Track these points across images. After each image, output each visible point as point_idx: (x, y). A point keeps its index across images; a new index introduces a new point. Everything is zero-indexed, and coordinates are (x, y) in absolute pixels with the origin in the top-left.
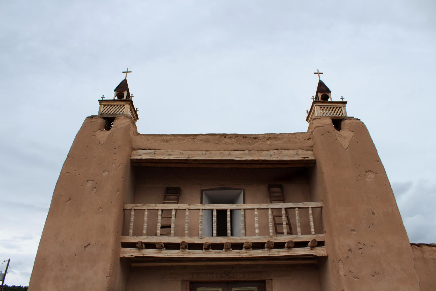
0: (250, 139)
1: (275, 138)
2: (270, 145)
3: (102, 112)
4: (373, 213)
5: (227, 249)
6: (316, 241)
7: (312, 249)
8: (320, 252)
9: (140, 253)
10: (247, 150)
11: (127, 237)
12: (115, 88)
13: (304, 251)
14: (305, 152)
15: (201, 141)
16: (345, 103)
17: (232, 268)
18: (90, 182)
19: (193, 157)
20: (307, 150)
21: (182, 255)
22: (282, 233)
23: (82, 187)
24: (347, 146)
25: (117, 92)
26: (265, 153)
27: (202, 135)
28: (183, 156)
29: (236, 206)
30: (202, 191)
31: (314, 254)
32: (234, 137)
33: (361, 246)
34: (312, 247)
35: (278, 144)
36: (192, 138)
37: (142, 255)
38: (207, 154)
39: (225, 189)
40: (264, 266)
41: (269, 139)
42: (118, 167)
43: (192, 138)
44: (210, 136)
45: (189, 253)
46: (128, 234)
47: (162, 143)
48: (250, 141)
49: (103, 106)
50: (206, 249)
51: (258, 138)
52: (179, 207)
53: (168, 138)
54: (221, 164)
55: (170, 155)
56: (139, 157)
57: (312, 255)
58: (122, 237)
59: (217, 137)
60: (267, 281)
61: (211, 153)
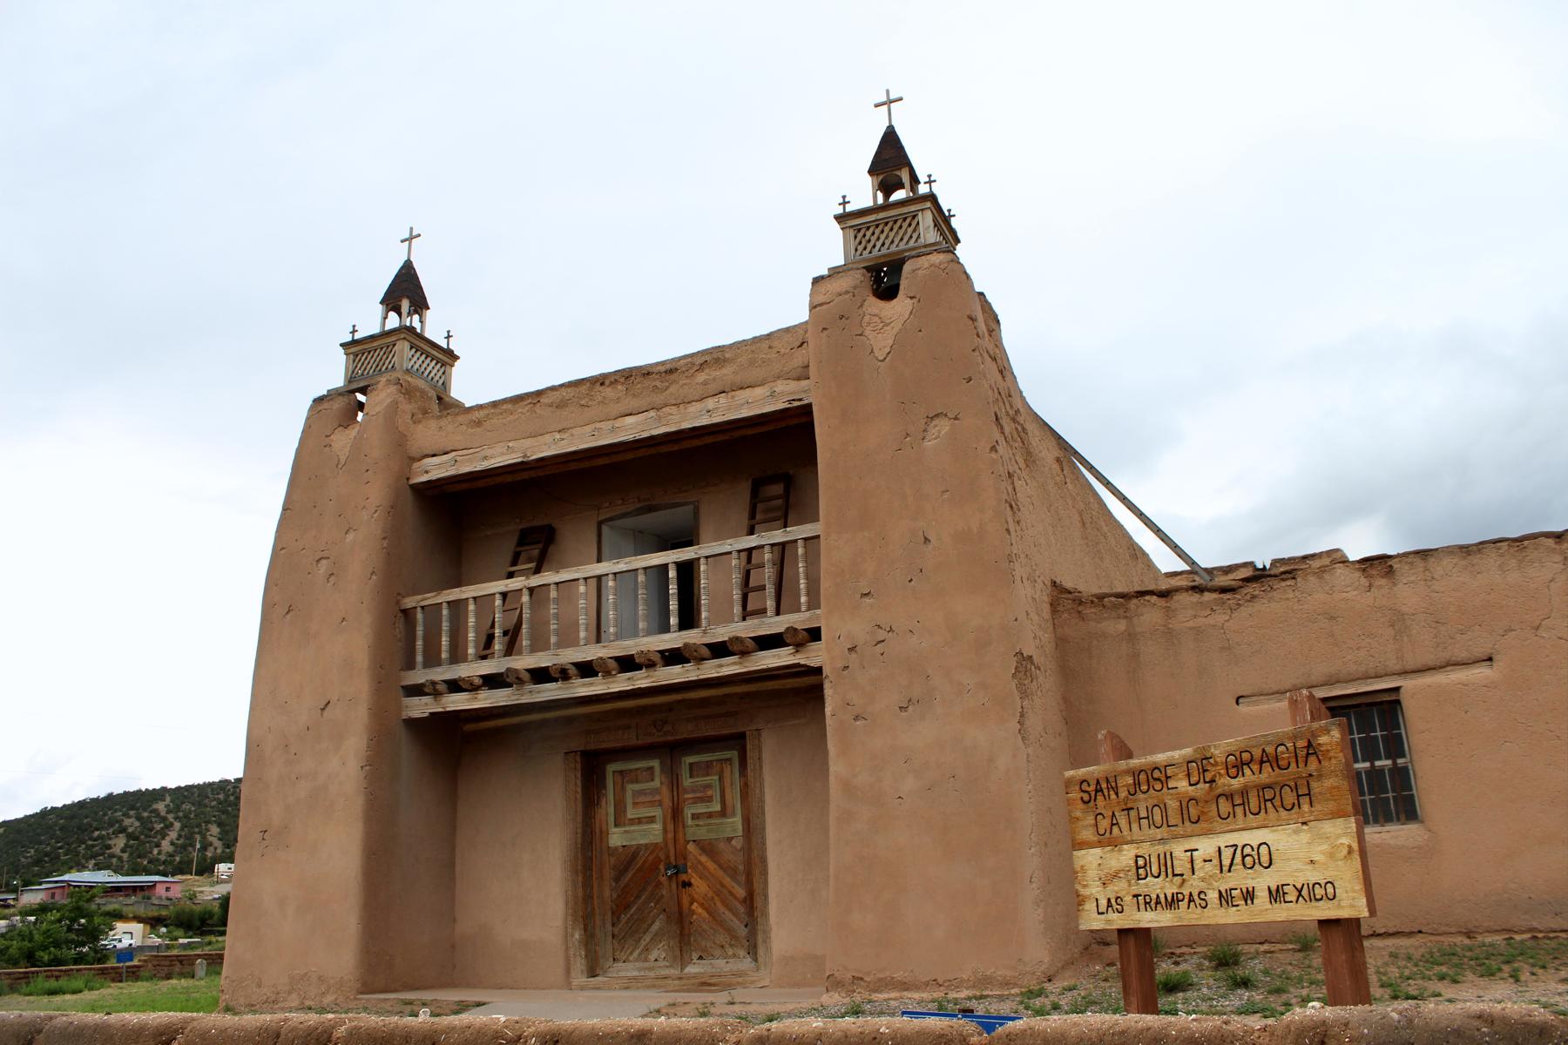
0: (658, 376)
1: (717, 360)
2: (705, 383)
3: (353, 372)
4: (926, 539)
5: (608, 673)
6: (796, 630)
7: (797, 651)
9: (438, 705)
10: (652, 409)
11: (411, 673)
12: (380, 300)
13: (779, 659)
14: (793, 386)
15: (550, 405)
17: (671, 710)
18: (324, 561)
19: (534, 453)
20: (799, 379)
21: (517, 700)
22: (762, 612)
23: (310, 576)
24: (887, 350)
25: (387, 305)
26: (694, 408)
27: (553, 389)
28: (514, 456)
29: (626, 563)
30: (600, 524)
31: (802, 662)
32: (622, 380)
33: (881, 635)
34: (799, 646)
35: (725, 375)
36: (530, 403)
37: (441, 710)
38: (563, 439)
39: (650, 509)
40: (743, 696)
41: (702, 367)
42: (372, 517)
43: (530, 403)
44: (569, 390)
45: (530, 692)
46: (410, 665)
47: (470, 430)
48: (658, 383)
49: (352, 356)
51: (676, 369)
52: (506, 586)
53: (482, 413)
54: (607, 455)
55: (485, 458)
56: (424, 478)
57: (798, 665)
58: (403, 673)
59: (583, 389)
60: (748, 733)
61: (572, 435)
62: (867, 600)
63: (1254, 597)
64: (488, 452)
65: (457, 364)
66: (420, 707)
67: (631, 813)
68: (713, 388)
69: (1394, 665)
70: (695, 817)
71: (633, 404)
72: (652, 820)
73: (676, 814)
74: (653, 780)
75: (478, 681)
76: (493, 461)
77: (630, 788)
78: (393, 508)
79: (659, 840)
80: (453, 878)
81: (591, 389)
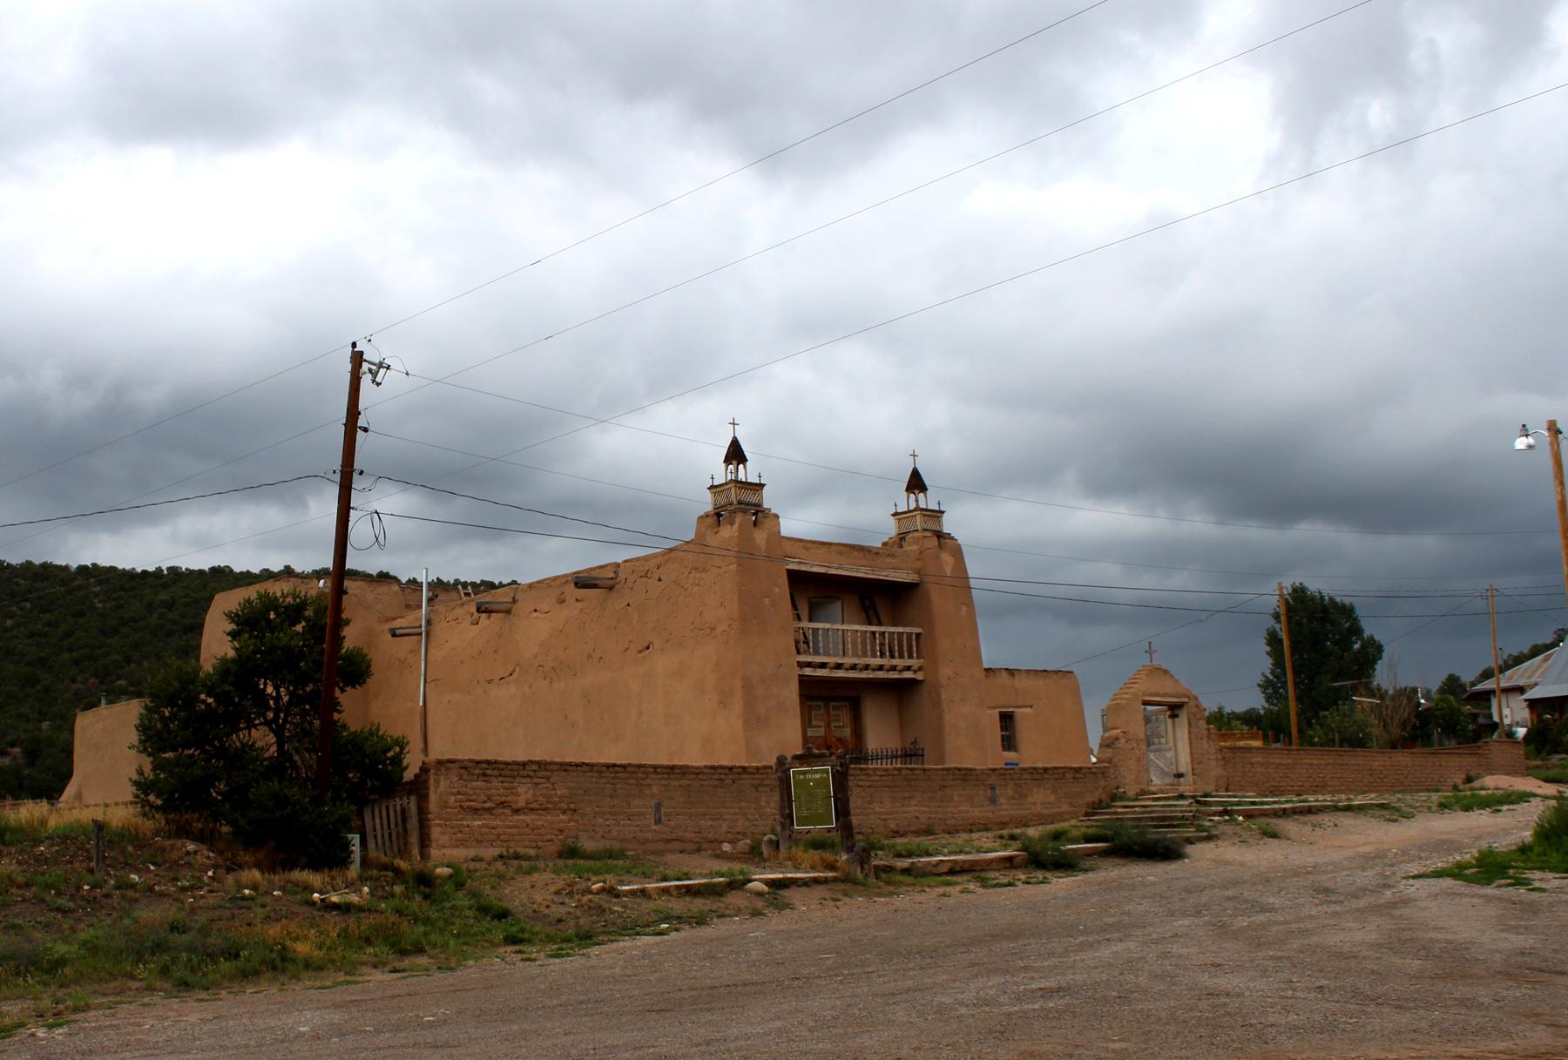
8: (919, 676)
16: (943, 512)
34: (915, 672)
50: (847, 669)
67: (814, 723)
68: (890, 566)
70: (835, 727)
71: (864, 562)
72: (820, 726)
73: (829, 725)
74: (820, 710)
77: (813, 713)
79: (823, 734)
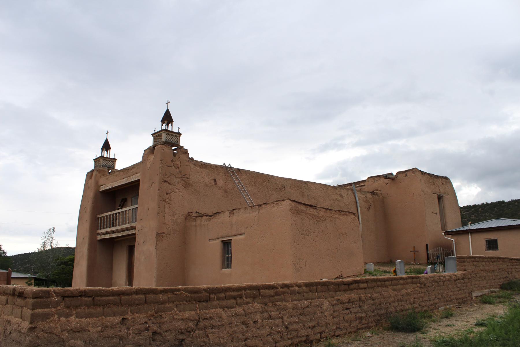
33: (142, 228)
46: (98, 229)
55: (108, 186)
62: (141, 221)
63: (213, 218)
64: (108, 185)
65: (117, 161)
66: (99, 238)
69: (230, 234)
71: (124, 176)
75: (104, 233)
76: (109, 187)
78: (96, 197)
80: (112, 271)
81: (120, 172)
